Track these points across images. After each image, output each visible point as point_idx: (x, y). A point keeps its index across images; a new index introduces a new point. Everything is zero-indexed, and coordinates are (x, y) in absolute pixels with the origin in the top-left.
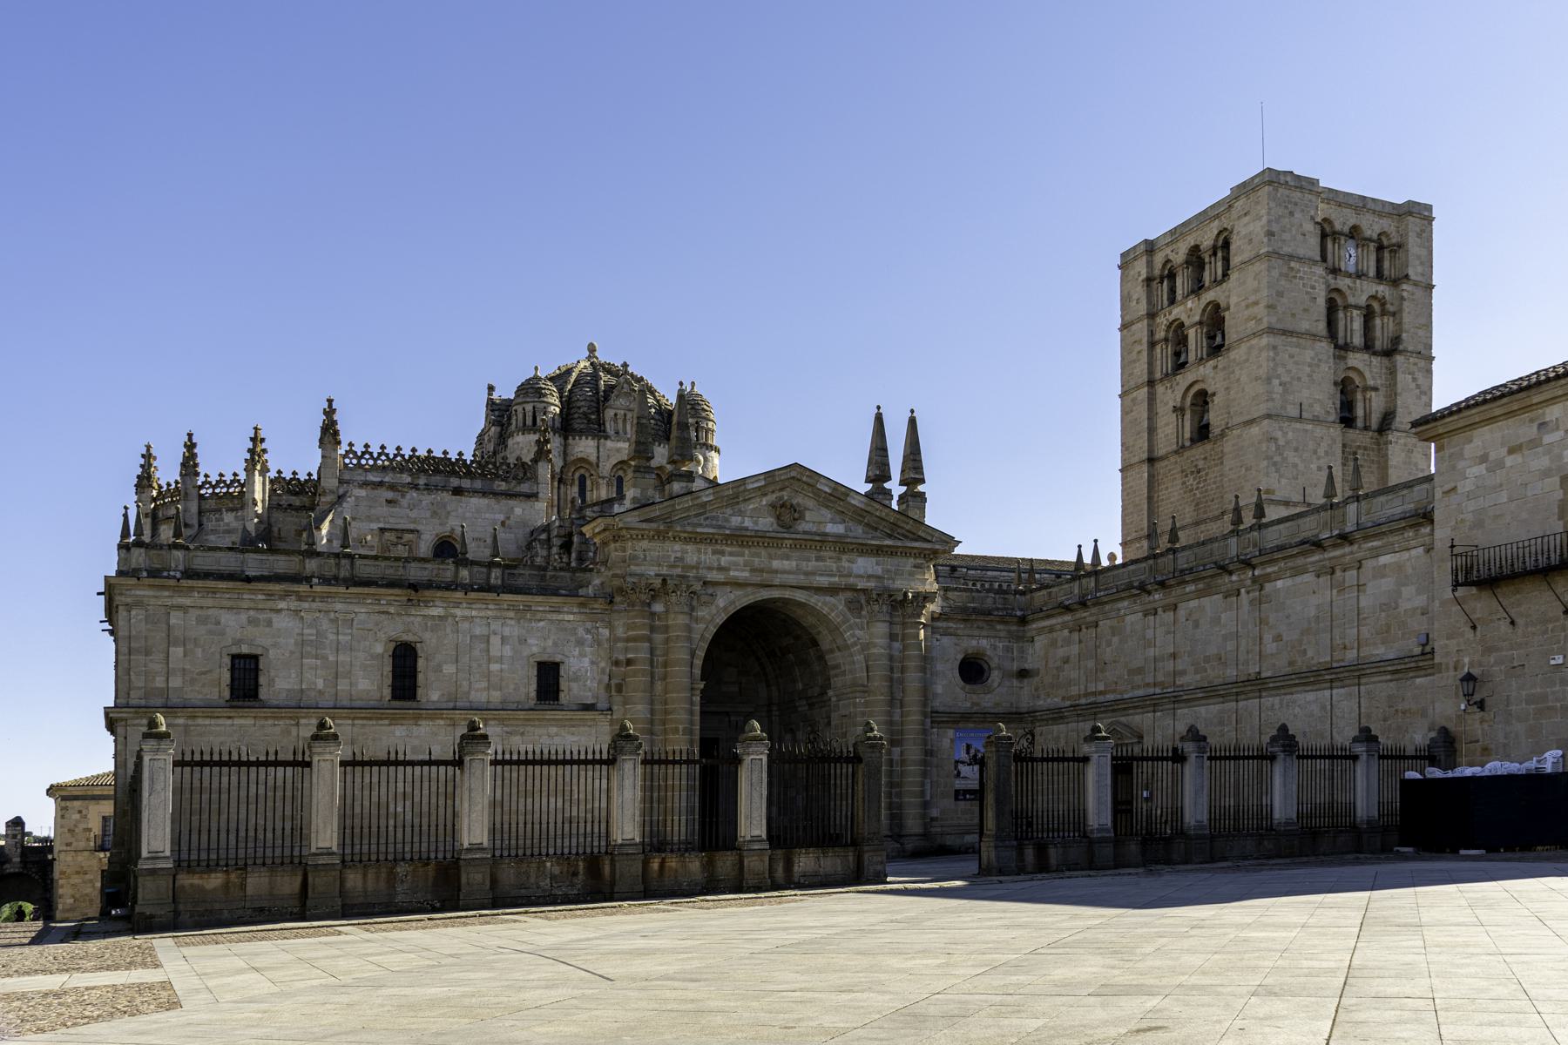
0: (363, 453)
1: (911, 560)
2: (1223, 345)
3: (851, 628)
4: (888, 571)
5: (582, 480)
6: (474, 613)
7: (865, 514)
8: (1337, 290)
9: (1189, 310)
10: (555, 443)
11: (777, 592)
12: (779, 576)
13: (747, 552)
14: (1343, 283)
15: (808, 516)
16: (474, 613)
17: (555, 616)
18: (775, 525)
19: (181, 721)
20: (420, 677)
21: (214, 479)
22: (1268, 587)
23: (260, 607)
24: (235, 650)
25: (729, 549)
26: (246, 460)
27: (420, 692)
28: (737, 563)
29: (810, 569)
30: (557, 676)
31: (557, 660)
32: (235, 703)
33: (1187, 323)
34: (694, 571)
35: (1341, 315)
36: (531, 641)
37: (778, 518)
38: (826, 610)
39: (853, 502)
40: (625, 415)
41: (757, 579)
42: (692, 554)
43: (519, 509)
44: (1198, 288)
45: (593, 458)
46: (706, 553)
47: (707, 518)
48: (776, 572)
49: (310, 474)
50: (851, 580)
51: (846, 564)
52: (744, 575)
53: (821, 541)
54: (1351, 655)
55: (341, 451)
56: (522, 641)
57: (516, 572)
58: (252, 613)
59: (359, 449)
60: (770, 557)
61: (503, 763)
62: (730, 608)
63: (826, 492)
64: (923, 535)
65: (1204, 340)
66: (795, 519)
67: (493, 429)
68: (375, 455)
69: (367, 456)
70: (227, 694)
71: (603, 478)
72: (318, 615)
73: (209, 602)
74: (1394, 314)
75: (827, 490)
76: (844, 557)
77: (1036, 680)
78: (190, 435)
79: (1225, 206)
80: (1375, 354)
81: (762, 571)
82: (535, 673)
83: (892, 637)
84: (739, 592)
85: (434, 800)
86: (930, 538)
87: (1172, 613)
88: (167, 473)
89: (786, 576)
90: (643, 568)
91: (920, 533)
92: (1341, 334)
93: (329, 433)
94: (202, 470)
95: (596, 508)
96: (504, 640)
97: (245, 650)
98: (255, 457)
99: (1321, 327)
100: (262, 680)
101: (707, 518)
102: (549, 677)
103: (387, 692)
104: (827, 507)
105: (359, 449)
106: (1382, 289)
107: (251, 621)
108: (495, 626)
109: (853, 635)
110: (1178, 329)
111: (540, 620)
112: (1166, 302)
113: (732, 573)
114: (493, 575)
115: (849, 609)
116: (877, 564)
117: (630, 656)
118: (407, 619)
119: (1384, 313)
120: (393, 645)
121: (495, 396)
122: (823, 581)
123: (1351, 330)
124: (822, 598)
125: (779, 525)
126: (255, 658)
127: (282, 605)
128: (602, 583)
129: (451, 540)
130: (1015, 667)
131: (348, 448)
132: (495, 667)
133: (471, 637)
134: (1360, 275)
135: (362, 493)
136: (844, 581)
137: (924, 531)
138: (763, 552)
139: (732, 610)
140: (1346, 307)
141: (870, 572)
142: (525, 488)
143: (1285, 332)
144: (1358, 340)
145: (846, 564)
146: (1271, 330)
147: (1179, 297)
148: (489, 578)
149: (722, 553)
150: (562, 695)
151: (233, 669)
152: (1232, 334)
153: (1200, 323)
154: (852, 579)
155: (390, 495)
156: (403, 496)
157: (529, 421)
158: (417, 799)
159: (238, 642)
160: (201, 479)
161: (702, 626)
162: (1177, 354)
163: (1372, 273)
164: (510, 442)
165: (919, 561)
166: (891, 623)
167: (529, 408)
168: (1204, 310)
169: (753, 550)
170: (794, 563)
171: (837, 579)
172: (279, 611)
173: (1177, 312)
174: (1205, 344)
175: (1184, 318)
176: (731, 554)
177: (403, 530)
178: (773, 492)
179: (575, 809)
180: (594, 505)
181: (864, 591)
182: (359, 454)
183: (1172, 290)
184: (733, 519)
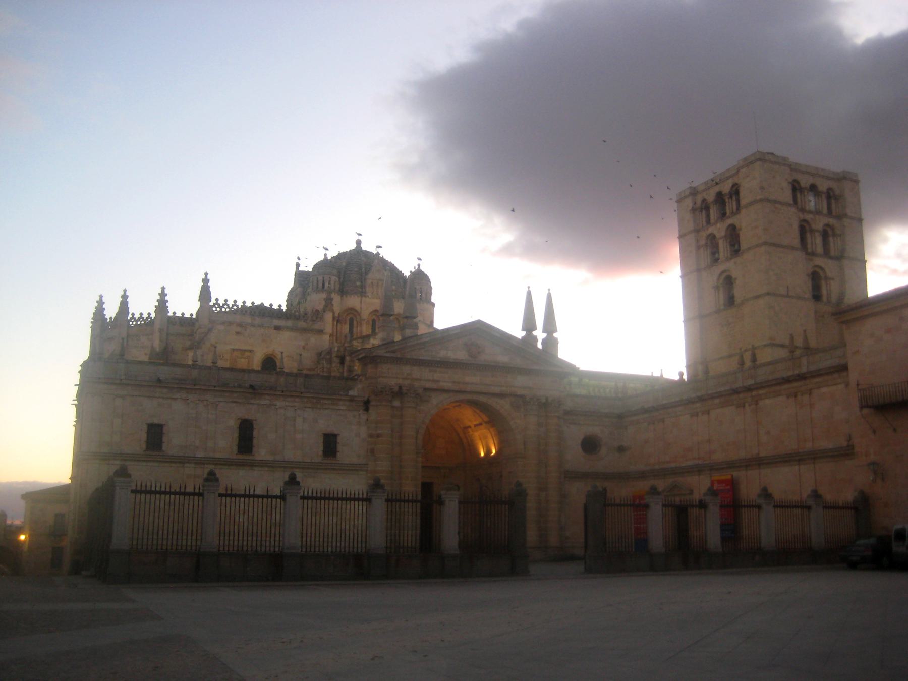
0: (224, 305)
2: (739, 250)
5: (351, 320)
8: (805, 221)
10: (336, 298)
14: (808, 217)
20: (255, 442)
21: (137, 316)
22: (761, 403)
24: (150, 421)
26: (156, 306)
27: (254, 450)
30: (336, 443)
31: (336, 432)
32: (148, 453)
33: (718, 236)
35: (808, 235)
40: (378, 283)
42: (416, 372)
43: (313, 340)
44: (723, 215)
45: (358, 308)
49: (191, 315)
54: (808, 446)
55: (211, 304)
59: (221, 302)
61: (308, 498)
65: (728, 246)
67: (298, 289)
68: (230, 306)
69: (226, 306)
70: (144, 446)
71: (364, 320)
72: (197, 402)
74: (840, 235)
78: (125, 291)
80: (831, 258)
82: (322, 440)
85: (260, 516)
88: (111, 312)
92: (809, 246)
93: (205, 293)
94: (131, 311)
95: (360, 341)
98: (162, 304)
99: (796, 242)
100: (165, 439)
102: (330, 444)
103: (235, 449)
105: (221, 302)
106: (832, 221)
110: (712, 237)
111: (326, 409)
112: (705, 223)
117: (379, 432)
119: (834, 235)
120: (240, 421)
121: (301, 269)
123: (815, 243)
126: (160, 426)
127: (178, 396)
129: (272, 357)
131: (215, 302)
134: (818, 212)
135: (222, 328)
140: (812, 231)
142: (317, 326)
143: (774, 245)
144: (820, 249)
146: (765, 243)
147: (712, 221)
150: (338, 455)
151: (148, 433)
152: (744, 245)
155: (239, 329)
156: (246, 330)
157: (320, 285)
158: (251, 514)
160: (130, 316)
162: (713, 254)
163: (825, 211)
164: (309, 298)
167: (320, 278)
172: (175, 399)
173: (711, 230)
174: (729, 249)
175: (715, 232)
177: (245, 350)
179: (343, 524)
180: (359, 338)
181: (522, 396)
182: (221, 305)
183: (708, 216)
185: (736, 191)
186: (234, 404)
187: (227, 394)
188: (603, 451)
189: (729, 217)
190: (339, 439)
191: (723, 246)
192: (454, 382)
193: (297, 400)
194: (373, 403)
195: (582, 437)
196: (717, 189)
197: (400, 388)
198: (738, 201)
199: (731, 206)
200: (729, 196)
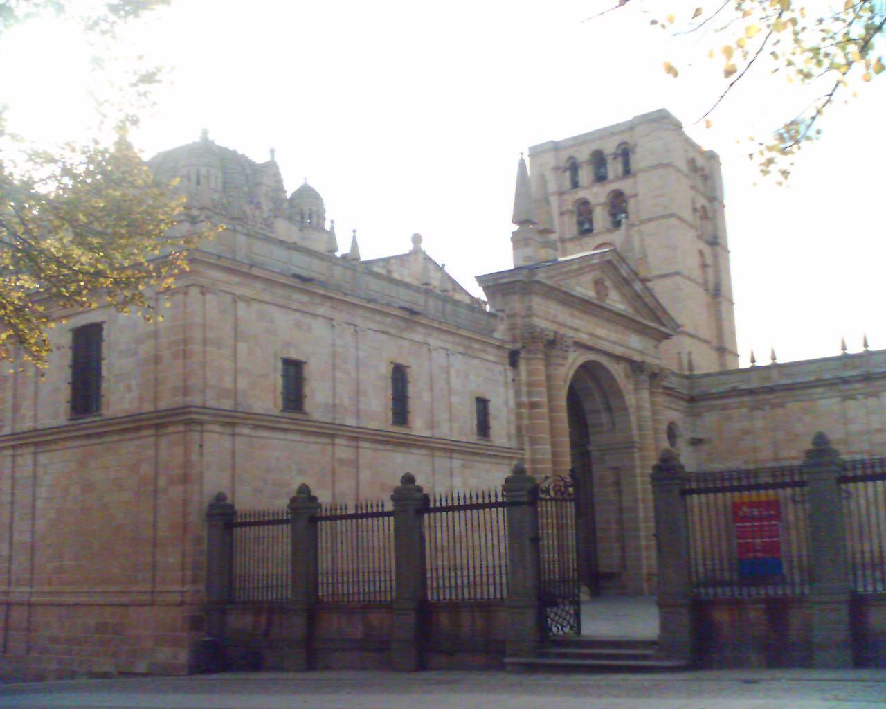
9: (597, 195)
19: (246, 431)
23: (305, 309)
27: (411, 417)
32: (288, 415)
33: (593, 201)
44: (601, 178)
52: (584, 338)
58: (298, 315)
73: (267, 297)
79: (631, 127)
97: (293, 355)
107: (298, 325)
117: (536, 399)
122: (619, 351)
127: (321, 311)
132: (454, 399)
153: (605, 204)
159: (288, 345)
162: (580, 223)
168: (609, 194)
185: (625, 153)
186: (384, 337)
187: (378, 318)
189: (613, 181)
191: (600, 217)
194: (522, 355)
196: (594, 146)
198: (626, 164)
199: (614, 168)
200: (612, 157)
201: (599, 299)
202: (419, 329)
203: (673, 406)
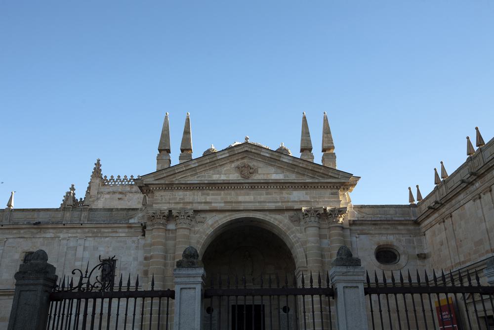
1: (329, 191)
3: (293, 232)
4: (314, 198)
6: (70, 235)
7: (294, 167)
11: (245, 214)
12: (242, 204)
13: (222, 192)
15: (260, 171)
16: (70, 235)
17: (114, 235)
18: (240, 178)
25: (212, 192)
28: (217, 199)
29: (262, 200)
34: (191, 205)
36: (101, 249)
37: (241, 173)
38: (276, 223)
39: (284, 160)
41: (229, 207)
46: (197, 195)
47: (199, 177)
48: (240, 202)
50: (290, 205)
51: (286, 196)
53: (267, 184)
56: (96, 248)
57: (96, 213)
60: (237, 195)
62: (215, 225)
63: (268, 157)
64: (332, 175)
66: (251, 173)
68: (115, 180)
75: (267, 155)
76: (284, 192)
77: (431, 259)
81: (231, 202)
83: (321, 237)
84: (221, 216)
86: (337, 177)
87: (489, 193)
89: (247, 204)
90: (160, 205)
91: (330, 174)
96: (85, 248)
101: (199, 177)
104: (271, 165)
108: (80, 242)
109: (295, 237)
111: (106, 237)
113: (213, 205)
114: (83, 215)
115: (292, 221)
116: (306, 194)
118: (34, 240)
122: (272, 206)
124: (273, 216)
125: (242, 177)
128: (143, 216)
130: (417, 252)
133: (67, 248)
135: (108, 196)
136: (284, 206)
137: (332, 173)
138: (233, 192)
139: (216, 226)
141: (302, 199)
145: (286, 196)
148: (81, 216)
149: (208, 195)
154: (290, 204)
155: (120, 196)
156: (126, 196)
161: (198, 235)
165: (335, 191)
166: (319, 228)
169: (226, 192)
170: (252, 197)
171: (280, 204)
176: (213, 195)
178: (237, 160)
184: (215, 176)
186: (22, 239)
187: (15, 231)
188: (403, 260)
190: (117, 264)
192: (225, 202)
193: (79, 231)
195: (376, 247)
197: (170, 211)
201: (244, 177)
202: (51, 231)
203: (390, 232)
